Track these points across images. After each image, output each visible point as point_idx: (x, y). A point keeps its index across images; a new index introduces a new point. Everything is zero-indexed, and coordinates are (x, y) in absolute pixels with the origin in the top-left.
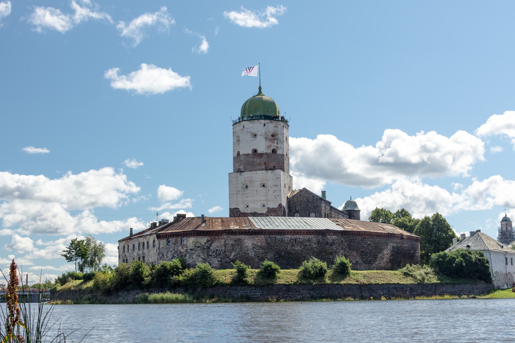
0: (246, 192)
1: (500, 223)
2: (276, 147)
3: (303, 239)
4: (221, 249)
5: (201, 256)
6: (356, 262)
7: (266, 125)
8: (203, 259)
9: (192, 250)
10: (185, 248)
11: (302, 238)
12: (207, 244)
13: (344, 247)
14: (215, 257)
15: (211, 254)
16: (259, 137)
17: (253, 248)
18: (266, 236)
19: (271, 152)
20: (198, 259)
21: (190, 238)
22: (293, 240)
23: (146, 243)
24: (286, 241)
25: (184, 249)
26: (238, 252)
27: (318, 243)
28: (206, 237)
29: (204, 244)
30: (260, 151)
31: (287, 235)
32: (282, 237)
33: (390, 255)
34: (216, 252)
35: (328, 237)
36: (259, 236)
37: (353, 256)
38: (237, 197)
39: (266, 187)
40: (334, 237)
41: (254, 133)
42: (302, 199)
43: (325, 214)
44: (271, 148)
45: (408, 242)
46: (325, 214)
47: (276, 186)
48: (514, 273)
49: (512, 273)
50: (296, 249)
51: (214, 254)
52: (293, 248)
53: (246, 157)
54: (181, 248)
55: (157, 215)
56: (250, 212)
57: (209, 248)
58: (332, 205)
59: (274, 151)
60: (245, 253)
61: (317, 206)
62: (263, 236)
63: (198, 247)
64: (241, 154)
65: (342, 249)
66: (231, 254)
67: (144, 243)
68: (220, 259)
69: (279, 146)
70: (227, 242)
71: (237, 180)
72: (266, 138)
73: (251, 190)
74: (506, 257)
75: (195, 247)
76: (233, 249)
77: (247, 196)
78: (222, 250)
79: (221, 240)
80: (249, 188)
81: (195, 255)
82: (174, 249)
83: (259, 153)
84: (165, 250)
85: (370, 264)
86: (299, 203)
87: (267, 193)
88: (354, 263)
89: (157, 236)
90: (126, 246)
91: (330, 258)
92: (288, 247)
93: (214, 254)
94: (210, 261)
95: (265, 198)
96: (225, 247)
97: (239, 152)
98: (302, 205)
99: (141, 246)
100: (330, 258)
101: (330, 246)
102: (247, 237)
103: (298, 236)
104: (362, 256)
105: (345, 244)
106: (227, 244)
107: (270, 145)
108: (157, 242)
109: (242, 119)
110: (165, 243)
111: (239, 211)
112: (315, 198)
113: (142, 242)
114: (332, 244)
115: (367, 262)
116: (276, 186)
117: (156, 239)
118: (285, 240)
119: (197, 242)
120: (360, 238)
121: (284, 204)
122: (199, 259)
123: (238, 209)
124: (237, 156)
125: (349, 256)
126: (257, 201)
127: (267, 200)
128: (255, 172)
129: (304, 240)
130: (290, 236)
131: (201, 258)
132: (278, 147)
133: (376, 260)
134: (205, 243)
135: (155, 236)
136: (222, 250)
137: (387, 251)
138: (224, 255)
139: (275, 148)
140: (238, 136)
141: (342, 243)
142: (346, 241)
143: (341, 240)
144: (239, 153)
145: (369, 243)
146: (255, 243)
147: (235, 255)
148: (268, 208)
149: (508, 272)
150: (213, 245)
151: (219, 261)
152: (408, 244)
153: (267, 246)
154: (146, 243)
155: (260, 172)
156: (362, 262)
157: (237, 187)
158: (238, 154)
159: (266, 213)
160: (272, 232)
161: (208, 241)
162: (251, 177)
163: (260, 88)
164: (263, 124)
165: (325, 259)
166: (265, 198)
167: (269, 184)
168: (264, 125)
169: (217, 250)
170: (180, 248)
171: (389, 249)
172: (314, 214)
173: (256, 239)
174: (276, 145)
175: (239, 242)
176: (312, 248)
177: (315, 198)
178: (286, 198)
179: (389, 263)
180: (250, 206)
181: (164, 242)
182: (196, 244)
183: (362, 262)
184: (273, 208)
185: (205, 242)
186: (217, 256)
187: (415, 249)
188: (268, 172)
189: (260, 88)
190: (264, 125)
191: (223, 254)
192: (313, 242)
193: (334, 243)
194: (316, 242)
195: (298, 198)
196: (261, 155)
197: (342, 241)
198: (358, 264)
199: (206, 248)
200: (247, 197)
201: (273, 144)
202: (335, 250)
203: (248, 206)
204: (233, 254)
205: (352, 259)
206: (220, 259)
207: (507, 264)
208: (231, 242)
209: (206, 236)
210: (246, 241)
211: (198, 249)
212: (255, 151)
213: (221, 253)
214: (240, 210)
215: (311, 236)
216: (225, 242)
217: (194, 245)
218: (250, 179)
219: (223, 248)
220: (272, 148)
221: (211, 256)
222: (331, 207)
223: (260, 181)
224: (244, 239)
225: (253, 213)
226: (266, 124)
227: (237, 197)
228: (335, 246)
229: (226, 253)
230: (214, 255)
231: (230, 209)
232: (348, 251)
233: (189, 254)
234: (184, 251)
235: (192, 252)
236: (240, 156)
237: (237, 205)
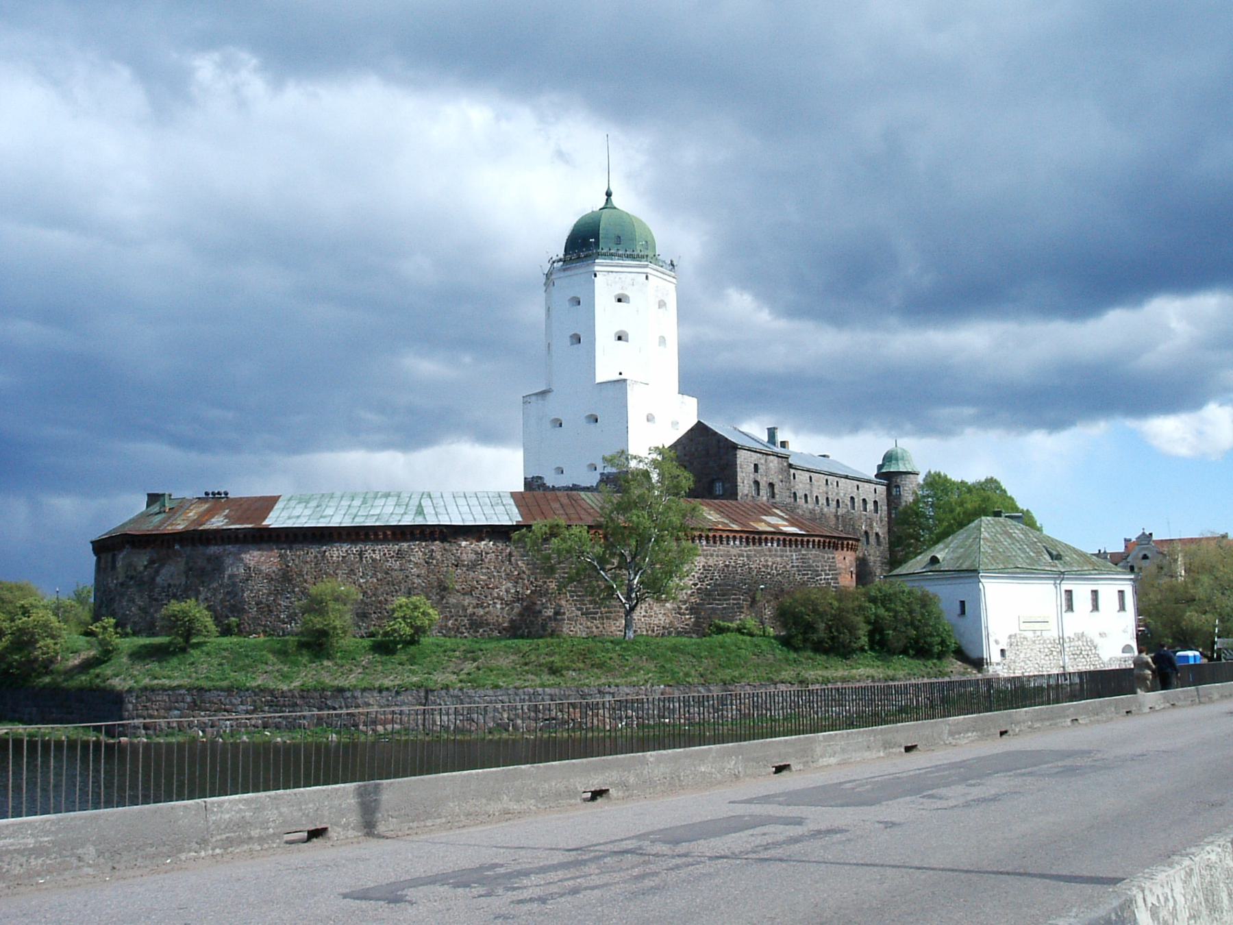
3: (382, 554)
11: (380, 550)
13: (516, 573)
15: (156, 596)
22: (354, 554)
24: (334, 558)
26: (214, 589)
27: (426, 562)
28: (149, 550)
29: (142, 568)
33: (689, 592)
35: (464, 543)
40: (483, 543)
42: (693, 450)
43: (757, 483)
45: (782, 550)
46: (757, 483)
49: (1092, 634)
50: (361, 581)
52: (353, 577)
57: (153, 579)
58: (791, 461)
61: (727, 465)
65: (509, 576)
70: (191, 564)
75: (127, 577)
78: (180, 584)
85: (608, 618)
86: (687, 458)
91: (466, 603)
92: (337, 575)
96: (187, 577)
98: (695, 463)
100: (466, 603)
101: (467, 570)
104: (577, 596)
105: (517, 564)
112: (722, 444)
114: (473, 566)
115: (597, 613)
118: (332, 557)
123: (540, 478)
129: (385, 554)
131: (137, 605)
134: (146, 567)
141: (510, 561)
143: (508, 551)
150: (163, 571)
152: (782, 556)
153: (280, 573)
156: (580, 612)
160: (296, 536)
161: (152, 562)
163: (609, 194)
165: (447, 607)
169: (169, 585)
176: (407, 577)
177: (722, 444)
179: (684, 614)
183: (580, 612)
185: (146, 563)
187: (818, 571)
189: (609, 194)
190: (595, 275)
192: (410, 561)
193: (482, 560)
194: (422, 561)
195: (685, 448)
197: (510, 554)
202: (484, 581)
207: (1070, 607)
209: (145, 548)
213: (179, 593)
215: (405, 545)
216: (187, 563)
222: (790, 466)
228: (484, 571)
231: (525, 478)
232: (526, 581)
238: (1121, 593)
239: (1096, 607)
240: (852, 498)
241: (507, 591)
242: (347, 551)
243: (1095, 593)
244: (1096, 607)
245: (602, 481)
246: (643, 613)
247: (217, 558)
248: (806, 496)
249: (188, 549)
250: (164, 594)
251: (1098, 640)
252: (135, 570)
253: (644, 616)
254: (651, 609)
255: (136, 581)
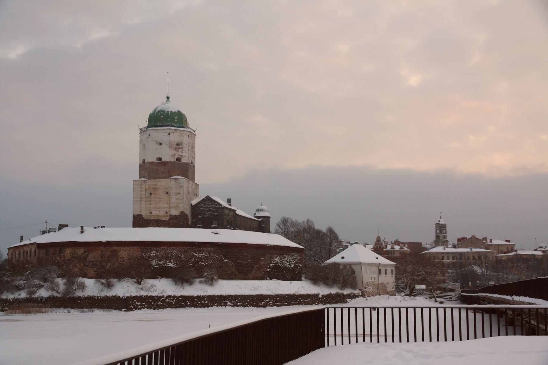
0: (150, 199)
1: (435, 226)
2: (180, 156)
4: (97, 260)
5: (77, 266)
6: (231, 272)
7: (170, 134)
8: (79, 269)
9: (69, 260)
10: (62, 259)
11: (177, 250)
12: (84, 255)
14: (92, 267)
15: (87, 264)
16: (163, 146)
17: (129, 259)
18: (142, 248)
19: (176, 161)
20: (74, 269)
21: (68, 249)
23: (29, 251)
25: (61, 259)
26: (114, 262)
29: (80, 254)
30: (164, 159)
31: (162, 247)
32: (158, 249)
34: (93, 263)
36: (135, 247)
37: (229, 266)
38: (141, 204)
39: (169, 195)
40: (210, 248)
41: (159, 142)
44: (176, 156)
47: (179, 194)
48: (388, 283)
49: (385, 282)
51: (91, 264)
53: (151, 165)
54: (59, 258)
55: (46, 223)
56: (153, 219)
57: (85, 259)
59: (178, 159)
60: (120, 264)
62: (139, 248)
63: (75, 258)
64: (146, 162)
66: (107, 265)
67: (27, 252)
68: (96, 270)
69: (184, 154)
71: (141, 188)
72: (170, 147)
73: (154, 197)
74: (380, 268)
75: (72, 257)
76: (109, 260)
77: (150, 203)
78: (98, 260)
79: (98, 251)
80: (153, 196)
81: (72, 265)
82: (52, 259)
83: (163, 161)
84: (44, 260)
85: (246, 274)
87: (170, 200)
88: (229, 273)
89: (37, 246)
90: (14, 254)
93: (91, 264)
94: (86, 271)
95: (166, 205)
96: (102, 257)
97: (144, 159)
99: (25, 254)
102: (124, 248)
103: (174, 248)
104: (237, 267)
106: (104, 255)
107: (174, 153)
108: (37, 251)
109: (149, 127)
110: (44, 253)
111: (143, 218)
113: (26, 251)
116: (179, 194)
117: (37, 249)
119: (75, 253)
120: (236, 250)
121: (188, 212)
122: (76, 269)
123: (141, 215)
124: (143, 164)
125: (224, 266)
126: (160, 208)
127: (170, 208)
128: (159, 180)
130: (165, 248)
132: (182, 156)
133: (252, 271)
134: (82, 254)
135: (36, 245)
136: (98, 260)
137: (265, 262)
138: (100, 265)
139: (180, 156)
140: (144, 145)
142: (222, 253)
144: (145, 161)
145: (245, 254)
146: (131, 254)
147: (111, 266)
148: (171, 215)
149: (382, 283)
151: (95, 271)
154: (29, 251)
155: (164, 180)
157: (141, 194)
158: (144, 161)
159: (168, 220)
161: (85, 252)
162: (155, 185)
164: (168, 133)
166: (166, 205)
167: (173, 191)
168: (169, 134)
170: (58, 258)
171: (267, 260)
172: (216, 221)
173: (132, 250)
174: (180, 153)
175: (115, 253)
178: (190, 206)
180: (154, 213)
181: (43, 252)
182: (73, 254)
184: (175, 215)
185: (82, 252)
186: (93, 266)
188: (172, 180)
189: (168, 98)
190: (169, 134)
191: (99, 264)
196: (165, 163)
198: (233, 274)
199: (82, 258)
200: (150, 204)
201: (177, 153)
203: (151, 213)
204: (109, 264)
205: (227, 269)
206: (96, 270)
207: (380, 273)
208: (108, 253)
210: (121, 252)
211: (75, 259)
212: (160, 159)
213: (98, 264)
214: (143, 217)
216: (102, 252)
217: (71, 256)
218: (155, 186)
219: (100, 259)
220: (177, 156)
221: (87, 266)
222: (236, 214)
223: (163, 189)
224: (120, 250)
225: (156, 220)
226: (170, 133)
227: (141, 204)
229: (103, 264)
230: (90, 266)
231: (134, 215)
233: (66, 264)
234: (61, 261)
235: (69, 262)
236: (145, 164)
237: (141, 211)
238: (392, 270)
239: (386, 274)
240: (250, 227)
241: (217, 265)
242: (166, 250)
243: (386, 270)
244: (386, 274)
245: (170, 218)
246: (255, 273)
247: (115, 251)
248: (239, 226)
249: (102, 248)
250: (91, 264)
251: (387, 286)
252: (77, 254)
253: (255, 274)
254: (257, 271)
255: (77, 259)
